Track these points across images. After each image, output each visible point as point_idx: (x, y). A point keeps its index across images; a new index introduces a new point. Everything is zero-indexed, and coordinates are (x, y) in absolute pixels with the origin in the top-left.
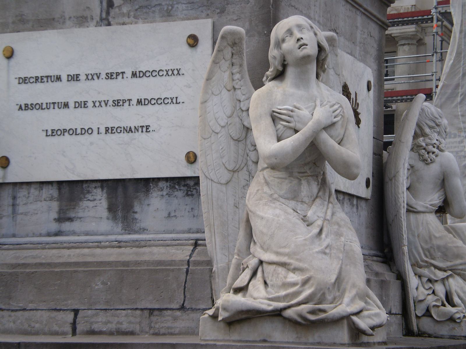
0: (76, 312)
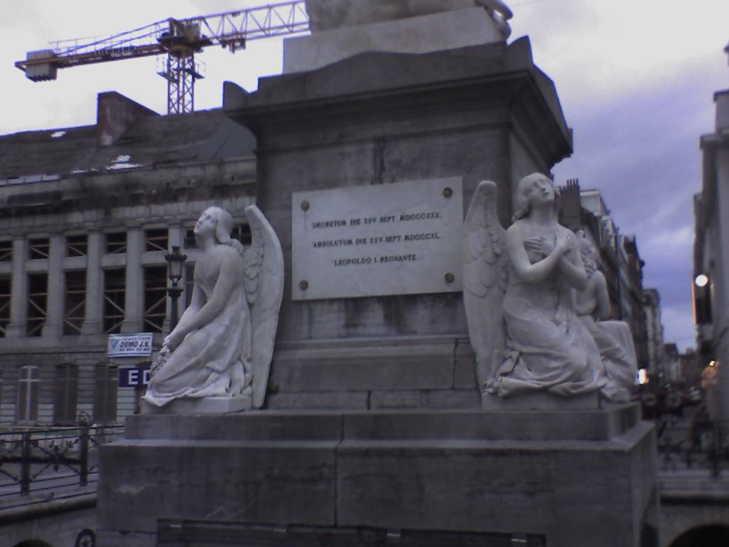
0: (369, 393)
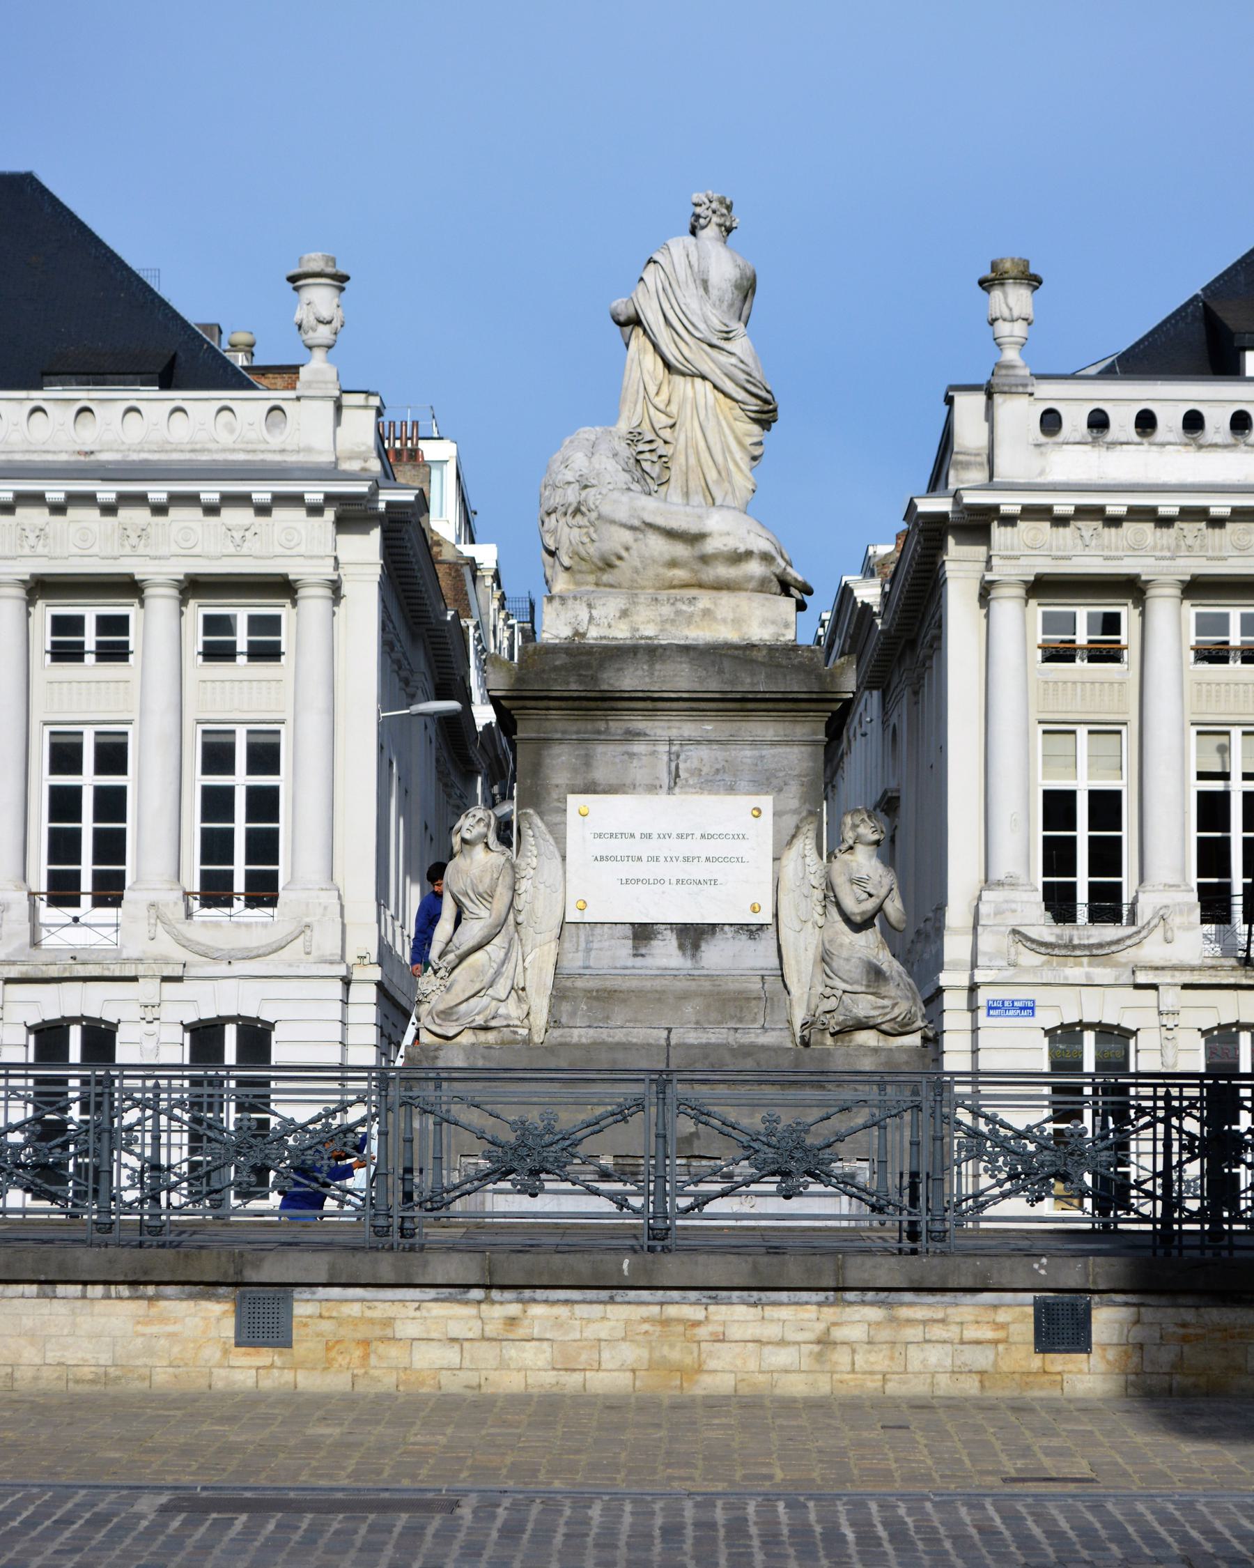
0: (669, 1030)
